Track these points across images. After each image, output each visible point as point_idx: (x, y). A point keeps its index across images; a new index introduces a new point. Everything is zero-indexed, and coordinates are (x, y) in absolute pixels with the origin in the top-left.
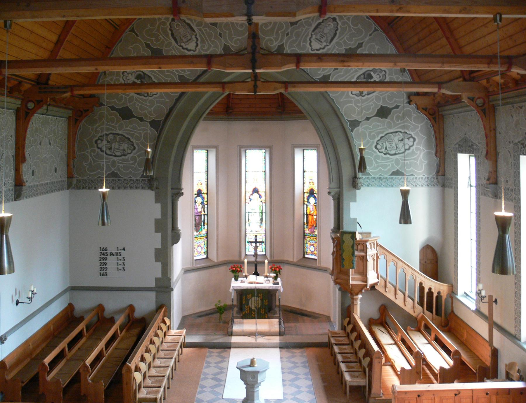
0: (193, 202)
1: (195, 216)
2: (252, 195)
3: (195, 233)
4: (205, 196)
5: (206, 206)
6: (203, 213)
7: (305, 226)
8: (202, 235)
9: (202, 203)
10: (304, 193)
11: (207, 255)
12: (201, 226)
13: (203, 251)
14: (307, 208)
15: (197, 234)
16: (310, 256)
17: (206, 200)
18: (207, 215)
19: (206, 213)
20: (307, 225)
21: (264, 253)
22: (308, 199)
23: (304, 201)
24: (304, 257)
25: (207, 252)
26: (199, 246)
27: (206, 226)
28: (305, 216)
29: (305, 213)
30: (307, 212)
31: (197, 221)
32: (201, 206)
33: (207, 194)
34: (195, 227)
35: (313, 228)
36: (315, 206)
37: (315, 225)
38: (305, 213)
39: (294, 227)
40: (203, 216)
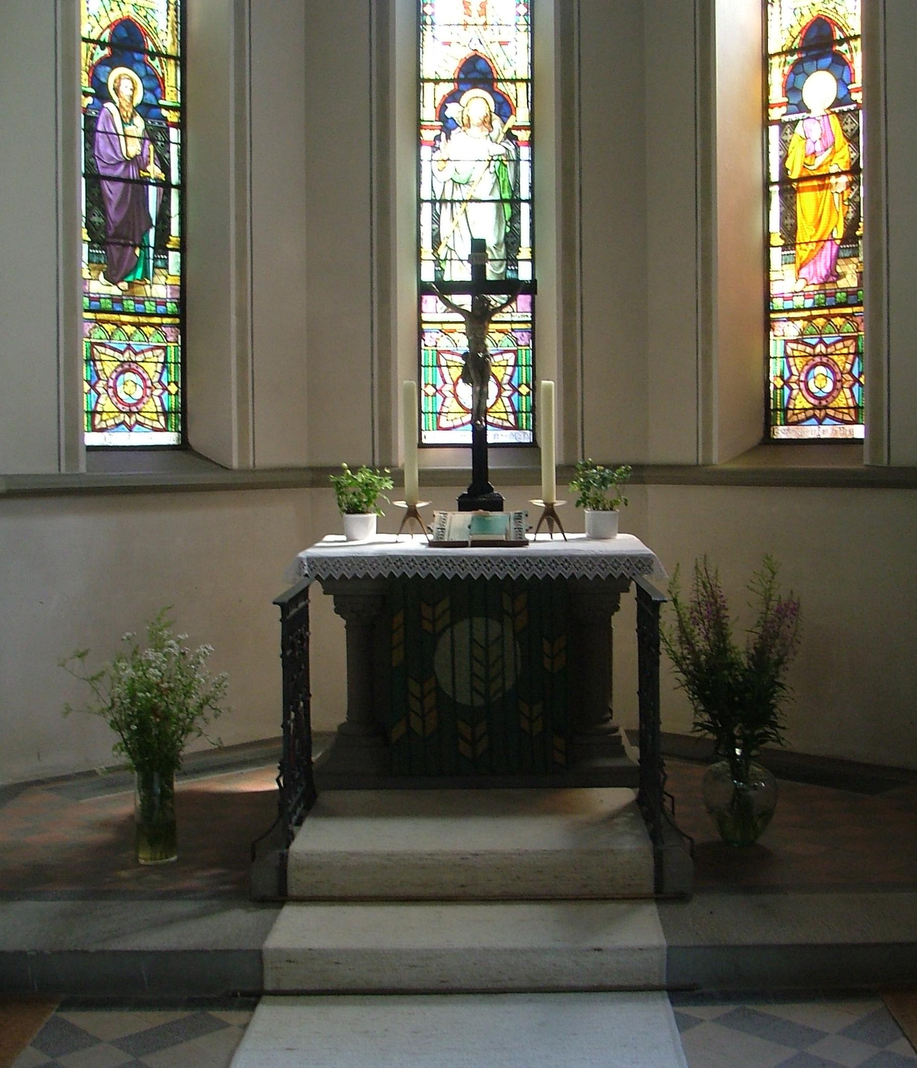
2: (454, 97)
3: (99, 286)
4: (171, 75)
5: (174, 134)
6: (154, 171)
7: (776, 255)
8: (150, 307)
9: (146, 109)
10: (766, 58)
11: (184, 434)
12: (144, 247)
13: (151, 406)
14: (784, 145)
15: (115, 291)
16: (811, 431)
17: (172, 97)
19: (175, 178)
21: (525, 437)
22: (792, 89)
23: (766, 106)
24: (768, 440)
25: (183, 411)
26: (126, 367)
27: (174, 258)
28: (775, 189)
29: (775, 176)
30: (784, 170)
32: (139, 126)
33: (182, 61)
38: (775, 176)
40: (153, 191)
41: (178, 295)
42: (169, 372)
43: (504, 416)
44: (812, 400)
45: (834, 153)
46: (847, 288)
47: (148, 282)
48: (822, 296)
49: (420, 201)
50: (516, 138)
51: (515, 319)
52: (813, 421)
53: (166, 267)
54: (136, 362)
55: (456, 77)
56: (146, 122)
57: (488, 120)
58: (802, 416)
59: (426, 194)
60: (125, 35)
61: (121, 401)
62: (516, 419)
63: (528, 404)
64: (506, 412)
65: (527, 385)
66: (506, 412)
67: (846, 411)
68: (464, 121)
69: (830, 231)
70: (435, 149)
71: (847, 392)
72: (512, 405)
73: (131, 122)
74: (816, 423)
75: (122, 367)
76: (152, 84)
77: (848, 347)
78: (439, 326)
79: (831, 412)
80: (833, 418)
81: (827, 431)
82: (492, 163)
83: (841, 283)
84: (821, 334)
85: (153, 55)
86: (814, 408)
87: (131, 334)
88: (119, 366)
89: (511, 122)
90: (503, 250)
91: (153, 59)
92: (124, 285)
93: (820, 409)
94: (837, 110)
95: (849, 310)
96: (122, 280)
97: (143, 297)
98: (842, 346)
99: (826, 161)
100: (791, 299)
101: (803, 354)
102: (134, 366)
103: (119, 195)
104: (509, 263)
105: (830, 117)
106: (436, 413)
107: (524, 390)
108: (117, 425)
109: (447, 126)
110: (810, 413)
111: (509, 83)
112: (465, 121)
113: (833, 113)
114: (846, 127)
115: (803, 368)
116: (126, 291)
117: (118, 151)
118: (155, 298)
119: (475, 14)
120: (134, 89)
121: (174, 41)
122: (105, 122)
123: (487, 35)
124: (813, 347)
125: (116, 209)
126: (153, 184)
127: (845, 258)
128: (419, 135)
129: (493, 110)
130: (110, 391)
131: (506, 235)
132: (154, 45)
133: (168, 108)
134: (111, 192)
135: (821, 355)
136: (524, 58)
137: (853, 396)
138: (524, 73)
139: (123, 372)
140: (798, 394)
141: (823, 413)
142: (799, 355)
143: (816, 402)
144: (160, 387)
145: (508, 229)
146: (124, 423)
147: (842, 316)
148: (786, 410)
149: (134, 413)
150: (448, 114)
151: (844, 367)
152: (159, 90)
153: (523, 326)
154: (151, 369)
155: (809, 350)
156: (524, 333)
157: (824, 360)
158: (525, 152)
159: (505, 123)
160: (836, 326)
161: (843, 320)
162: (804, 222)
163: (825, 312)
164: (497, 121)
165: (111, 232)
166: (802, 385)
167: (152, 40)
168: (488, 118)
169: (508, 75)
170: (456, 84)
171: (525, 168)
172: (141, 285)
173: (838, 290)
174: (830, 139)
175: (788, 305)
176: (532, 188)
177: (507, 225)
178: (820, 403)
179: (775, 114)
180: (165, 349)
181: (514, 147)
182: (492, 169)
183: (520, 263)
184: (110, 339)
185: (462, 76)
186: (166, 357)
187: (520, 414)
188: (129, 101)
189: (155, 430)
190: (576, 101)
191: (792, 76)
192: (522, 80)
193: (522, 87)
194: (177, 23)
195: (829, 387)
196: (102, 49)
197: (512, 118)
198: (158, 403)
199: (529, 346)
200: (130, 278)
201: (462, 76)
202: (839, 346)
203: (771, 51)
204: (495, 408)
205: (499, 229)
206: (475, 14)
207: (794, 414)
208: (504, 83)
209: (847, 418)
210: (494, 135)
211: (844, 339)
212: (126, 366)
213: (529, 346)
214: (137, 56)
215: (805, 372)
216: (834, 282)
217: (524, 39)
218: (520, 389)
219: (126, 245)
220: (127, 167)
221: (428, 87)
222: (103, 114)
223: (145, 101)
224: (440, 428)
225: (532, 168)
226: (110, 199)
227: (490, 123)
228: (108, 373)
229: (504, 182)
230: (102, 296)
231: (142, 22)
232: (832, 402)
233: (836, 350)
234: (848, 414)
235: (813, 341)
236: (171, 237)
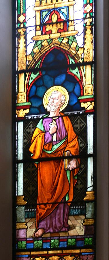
7: (21, 212)
45: (67, 143)
46: (76, 236)
48: (56, 241)
69: (63, 196)
83: (72, 233)
94: (69, 113)
99: (61, 148)
100: (33, 242)
105: (64, 118)
113: (66, 115)
161: (73, 257)
162: (43, 189)
163: (59, 252)
173: (69, 237)
174: (64, 133)
175: (31, 246)
191: (34, 88)
216: (66, 232)
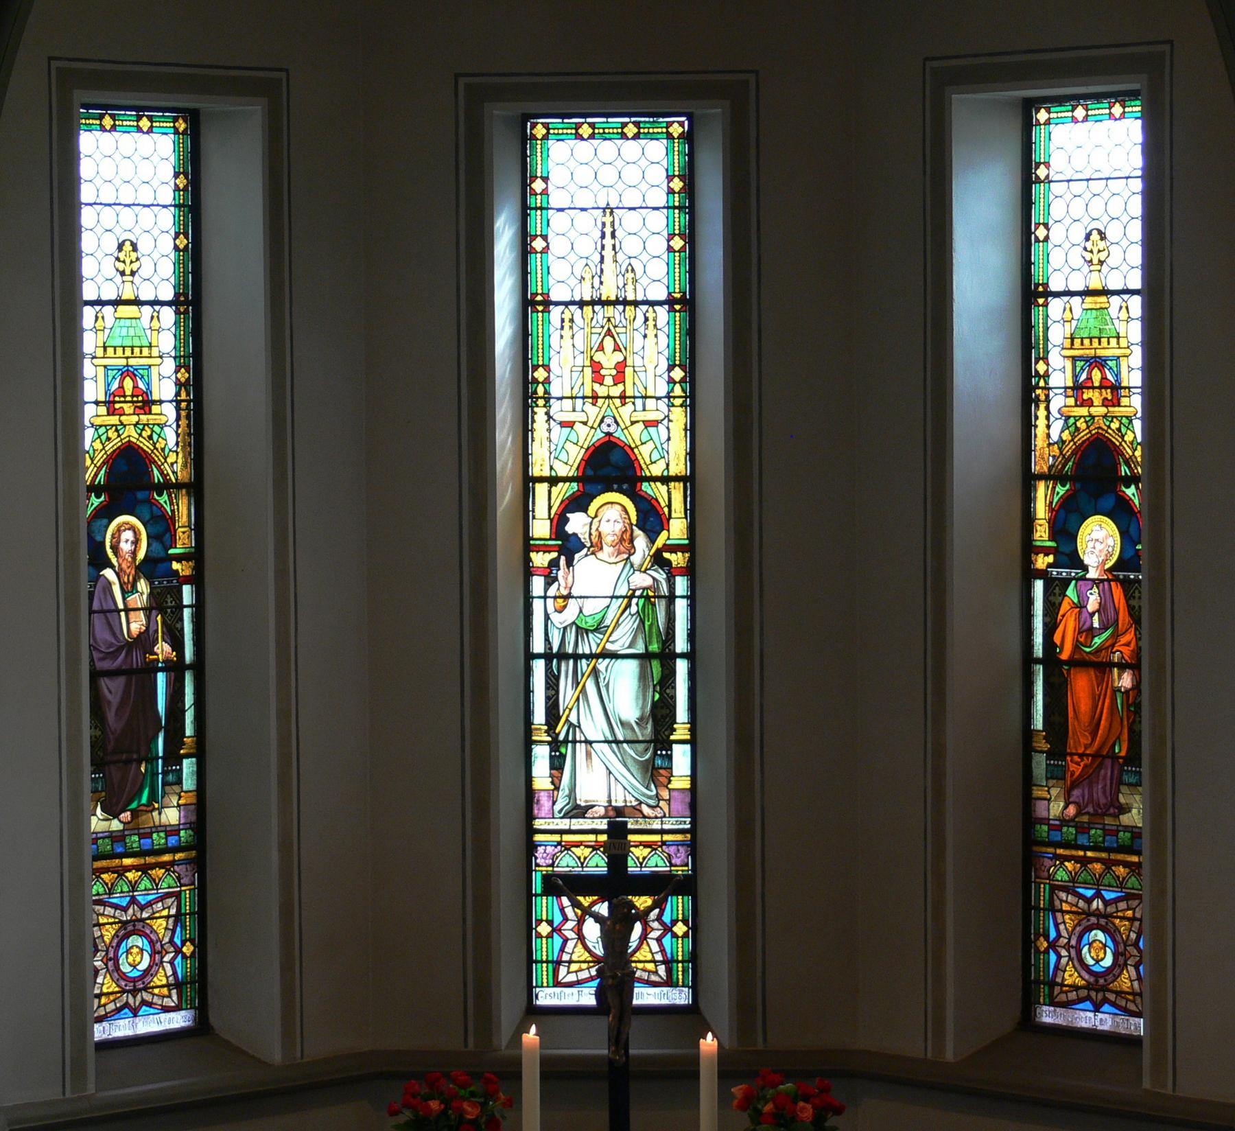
0: (72, 548)
1: (95, 675)
3: (98, 822)
4: (183, 510)
6: (163, 649)
7: (1040, 763)
8: (158, 839)
9: (152, 567)
12: (151, 760)
15: (116, 825)
16: (1085, 1018)
17: (183, 541)
18: (198, 667)
20: (1058, 751)
23: (1029, 549)
26: (129, 929)
27: (188, 766)
29: (1038, 651)
31: (111, 716)
34: (97, 765)
35: (1106, 772)
36: (1126, 584)
37: (1121, 750)
38: (1038, 651)
39: (939, 775)
41: (193, 818)
42: (184, 927)
43: (651, 966)
44: (1087, 977)
45: (1116, 636)
46: (1132, 827)
47: (156, 805)
48: (1099, 832)
49: (530, 656)
50: (668, 563)
51: (666, 827)
52: (1088, 1005)
53: (179, 782)
54: (143, 920)
55: (580, 474)
56: (151, 584)
57: (627, 536)
58: (1073, 996)
59: (538, 646)
60: (125, 468)
61: (123, 976)
62: (669, 971)
63: (686, 949)
64: (654, 961)
65: (685, 922)
66: (654, 961)
67: (1130, 997)
68: (593, 537)
69: (1111, 743)
70: (550, 580)
71: (1132, 969)
72: (663, 951)
73: (134, 589)
74: (1091, 1008)
75: (125, 929)
76: (159, 528)
77: (1134, 910)
78: (557, 838)
79: (1112, 997)
80: (1113, 1004)
81: (1104, 1021)
82: (634, 601)
83: (1125, 819)
84: (1098, 885)
85: (160, 488)
86: (1088, 987)
87: (136, 882)
88: (120, 928)
89: (661, 541)
90: (649, 726)
91: (160, 495)
92: (126, 816)
93: (1097, 991)
94: (1121, 575)
95: (1135, 859)
96: (124, 811)
97: (151, 828)
98: (1125, 907)
99: (1107, 645)
100: (1059, 828)
101: (1074, 909)
102: (139, 926)
103: (120, 694)
104: (659, 746)
105: (1113, 584)
106: (552, 962)
107: (680, 929)
108: (119, 1010)
109: (568, 547)
110: (1083, 993)
111: (658, 484)
112: (595, 539)
113: (1116, 579)
114: (1132, 602)
115: (1074, 929)
116: (129, 823)
117: (118, 632)
118: (165, 826)
119: (608, 381)
120: (136, 542)
121: (186, 462)
122: (102, 597)
123: (626, 412)
124: (1089, 901)
125: (116, 714)
126: (161, 670)
127: (1129, 785)
128: (528, 560)
129: (634, 522)
130: (110, 963)
131: (654, 705)
132: (162, 472)
133: (179, 558)
134: (110, 692)
135: (1097, 914)
136: (679, 446)
137: (1139, 978)
138: (679, 467)
139: (127, 936)
140: (1067, 964)
141: (1100, 996)
142: (1069, 909)
143: (1092, 980)
144: (172, 949)
145: (657, 696)
146: (126, 1005)
147: (1126, 864)
148: (1052, 984)
149: (140, 990)
150: (570, 528)
151: (1129, 935)
152: (168, 535)
153: (679, 837)
154: (160, 925)
155: (1081, 903)
156: (680, 847)
157: (1103, 922)
158: (681, 584)
159: (653, 543)
160: (1118, 877)
161: (1127, 870)
162: (1076, 723)
163: (1104, 855)
164: (641, 541)
165: (110, 748)
166: (1073, 952)
167: (159, 467)
168: (628, 534)
169: (657, 470)
170: (581, 484)
171: (681, 607)
172: (147, 811)
173: (1120, 828)
174: (1111, 613)
175: (1056, 836)
176: (692, 636)
177: (654, 691)
178: (1097, 981)
179: (1042, 562)
180: (178, 895)
181: (665, 576)
182: (634, 609)
183: (675, 746)
184: (110, 894)
185: (590, 472)
186: (179, 908)
187: (675, 965)
188: (130, 559)
189: (166, 1009)
190: (756, 526)
191: (1062, 512)
192: (677, 479)
193: (677, 491)
194: (189, 435)
195: (1108, 962)
196: (98, 497)
197: (664, 534)
198: (169, 972)
199: (687, 865)
200: (134, 805)
201: (590, 472)
202: (1122, 905)
203: (1036, 469)
204: (638, 956)
205: (644, 700)
206: (608, 381)
207: (1062, 992)
208: (652, 484)
209: (1132, 1007)
210: (636, 559)
211: (1128, 897)
212: (130, 928)
213: (687, 865)
214: (140, 495)
215: (1077, 935)
216: (1116, 816)
217: (679, 417)
218: (675, 929)
219: (128, 762)
220: (129, 654)
221: (541, 489)
222: (99, 585)
223: (149, 554)
224: (557, 984)
225: (692, 607)
226: (109, 703)
227: (632, 541)
228: (107, 939)
229: (650, 627)
230: (99, 835)
231: (146, 445)
232: (1112, 982)
233: (1118, 911)
234: (1134, 1002)
235: (1089, 893)
236: (185, 739)
